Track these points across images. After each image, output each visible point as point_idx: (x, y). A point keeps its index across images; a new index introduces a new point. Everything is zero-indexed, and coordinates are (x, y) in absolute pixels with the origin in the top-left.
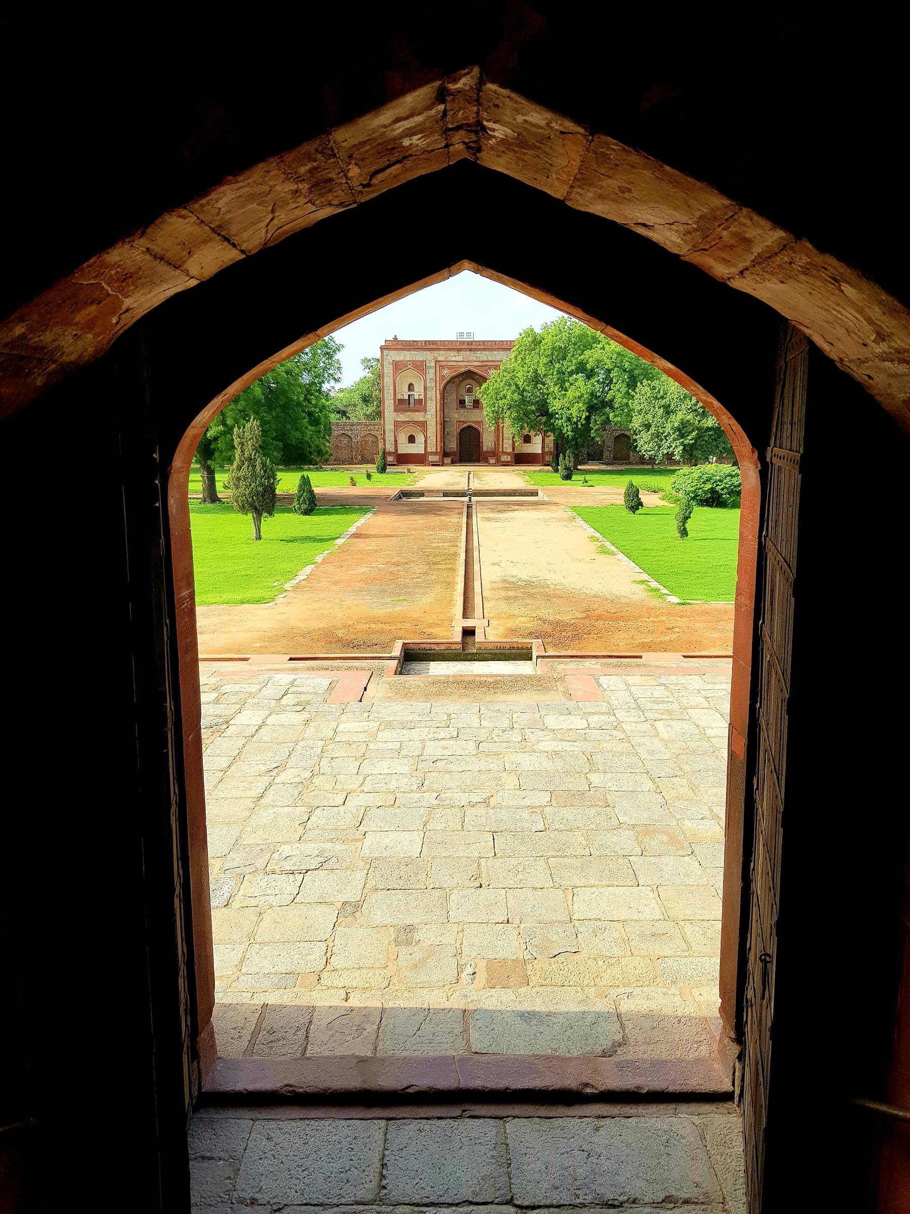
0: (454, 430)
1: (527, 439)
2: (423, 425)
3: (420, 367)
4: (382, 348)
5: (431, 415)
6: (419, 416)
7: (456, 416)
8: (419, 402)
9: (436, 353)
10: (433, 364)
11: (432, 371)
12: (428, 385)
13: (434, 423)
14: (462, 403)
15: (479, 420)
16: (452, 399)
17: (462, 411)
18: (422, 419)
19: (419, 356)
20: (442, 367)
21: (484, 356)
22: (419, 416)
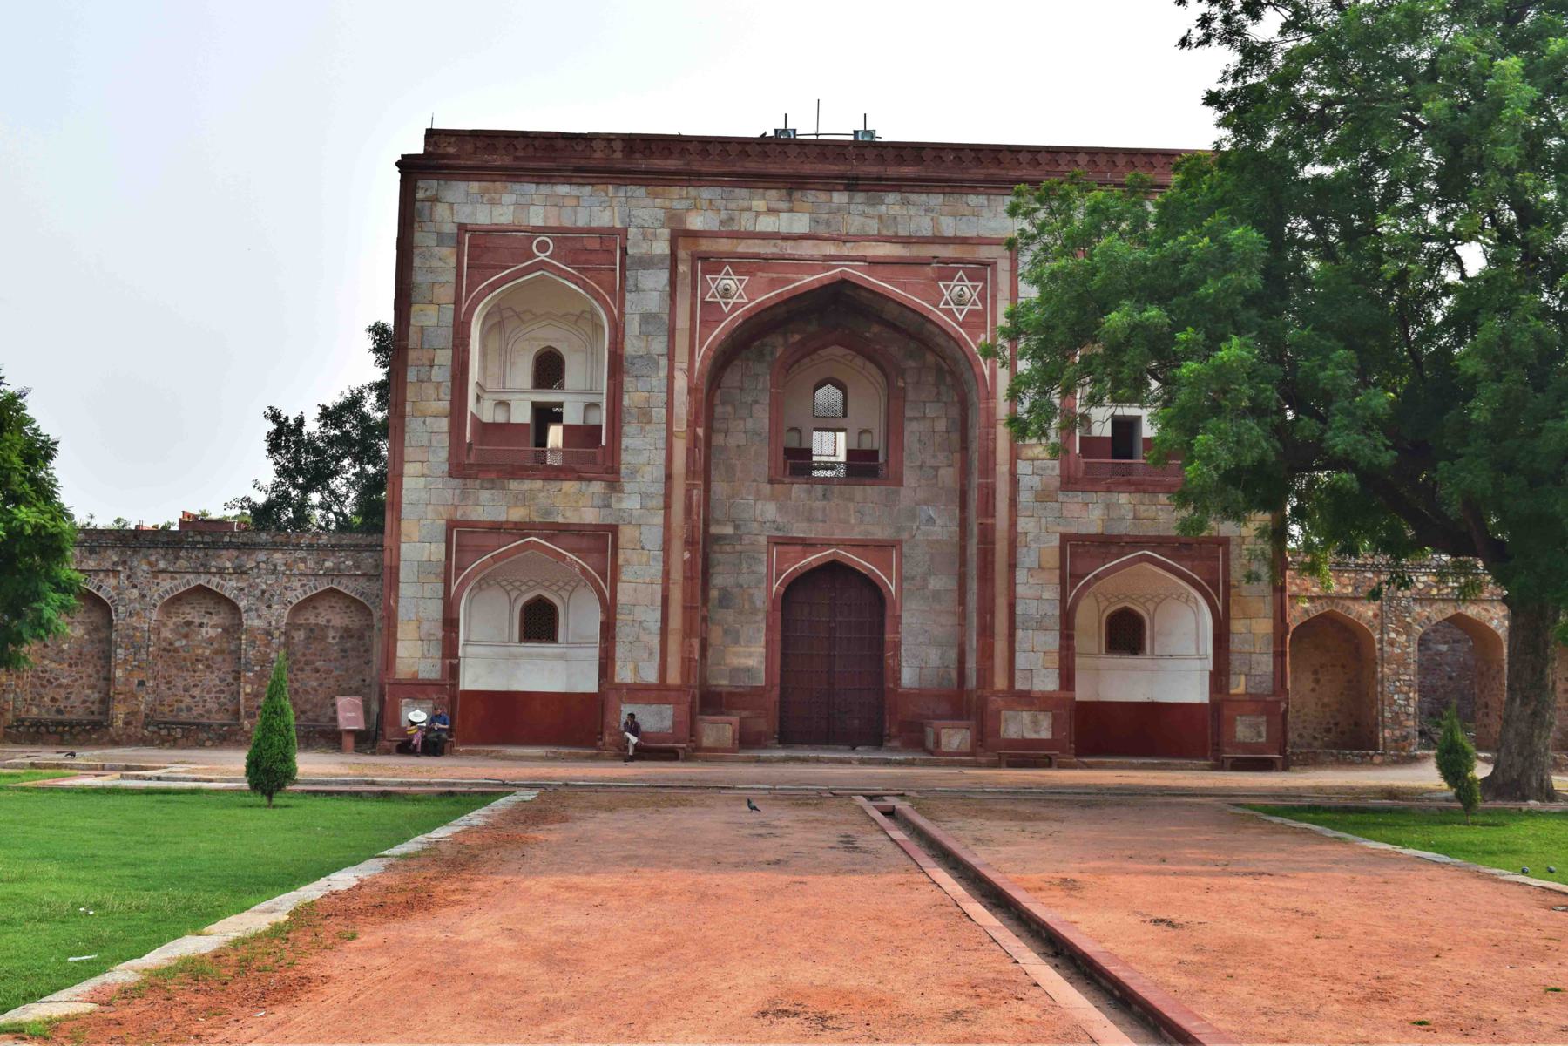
0: (757, 582)
1: (1126, 634)
2: (601, 542)
3: (598, 258)
4: (408, 165)
5: (641, 503)
6: (577, 503)
7: (770, 511)
8: (582, 436)
9: (677, 198)
10: (662, 247)
11: (657, 280)
12: (632, 346)
13: (652, 536)
14: (798, 461)
15: (880, 533)
16: (749, 429)
17: (798, 490)
18: (590, 516)
19: (592, 207)
20: (713, 263)
21: (923, 214)
22: (577, 503)
